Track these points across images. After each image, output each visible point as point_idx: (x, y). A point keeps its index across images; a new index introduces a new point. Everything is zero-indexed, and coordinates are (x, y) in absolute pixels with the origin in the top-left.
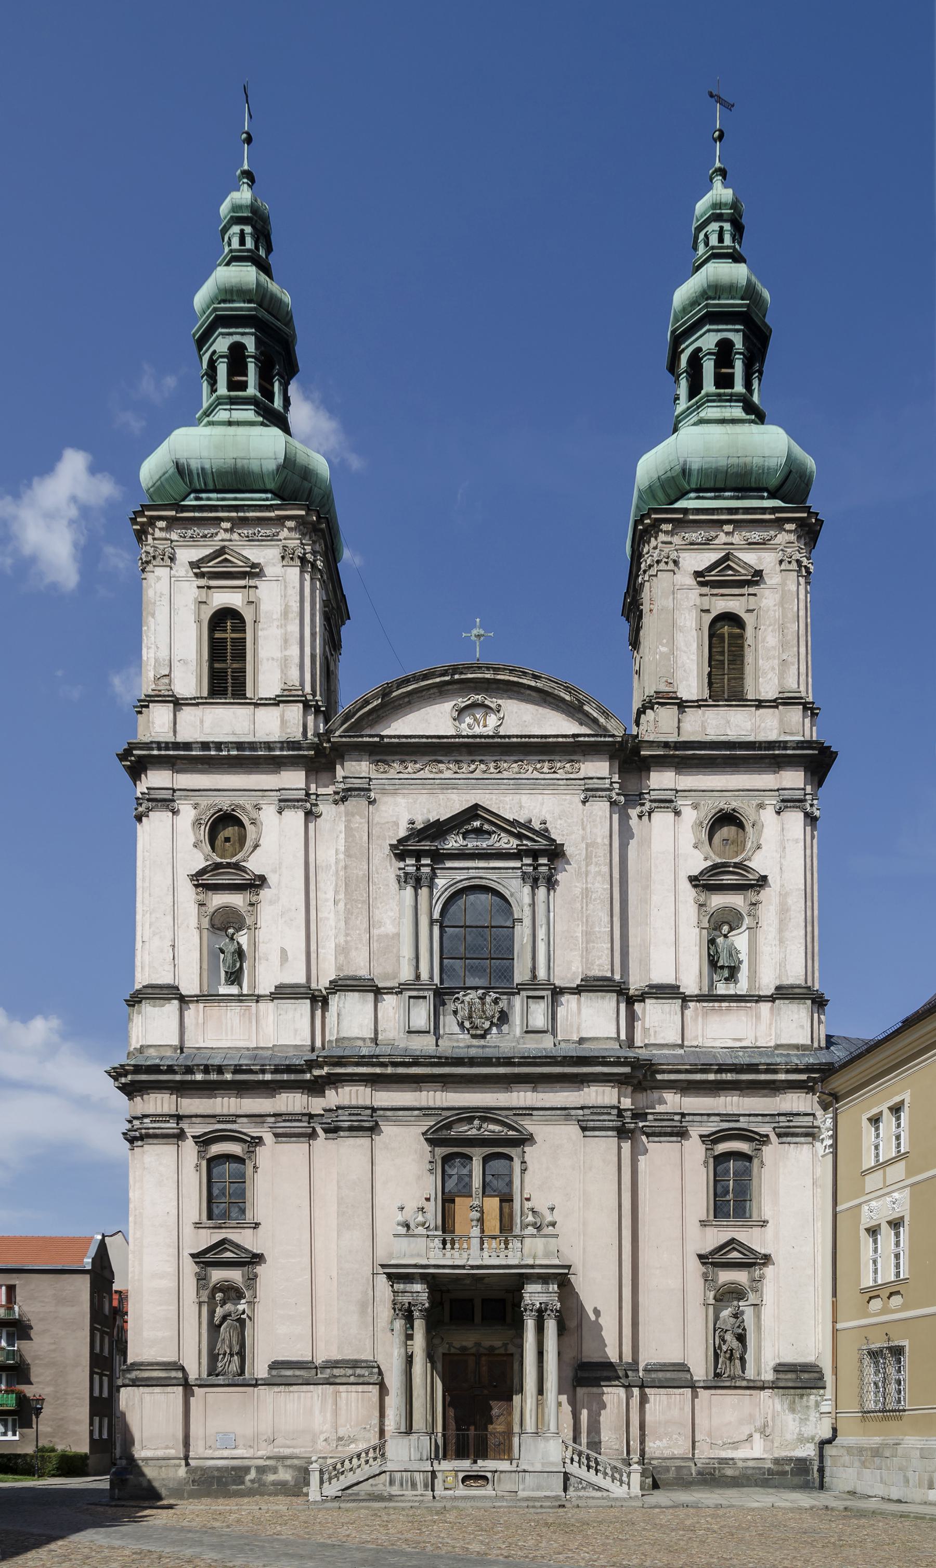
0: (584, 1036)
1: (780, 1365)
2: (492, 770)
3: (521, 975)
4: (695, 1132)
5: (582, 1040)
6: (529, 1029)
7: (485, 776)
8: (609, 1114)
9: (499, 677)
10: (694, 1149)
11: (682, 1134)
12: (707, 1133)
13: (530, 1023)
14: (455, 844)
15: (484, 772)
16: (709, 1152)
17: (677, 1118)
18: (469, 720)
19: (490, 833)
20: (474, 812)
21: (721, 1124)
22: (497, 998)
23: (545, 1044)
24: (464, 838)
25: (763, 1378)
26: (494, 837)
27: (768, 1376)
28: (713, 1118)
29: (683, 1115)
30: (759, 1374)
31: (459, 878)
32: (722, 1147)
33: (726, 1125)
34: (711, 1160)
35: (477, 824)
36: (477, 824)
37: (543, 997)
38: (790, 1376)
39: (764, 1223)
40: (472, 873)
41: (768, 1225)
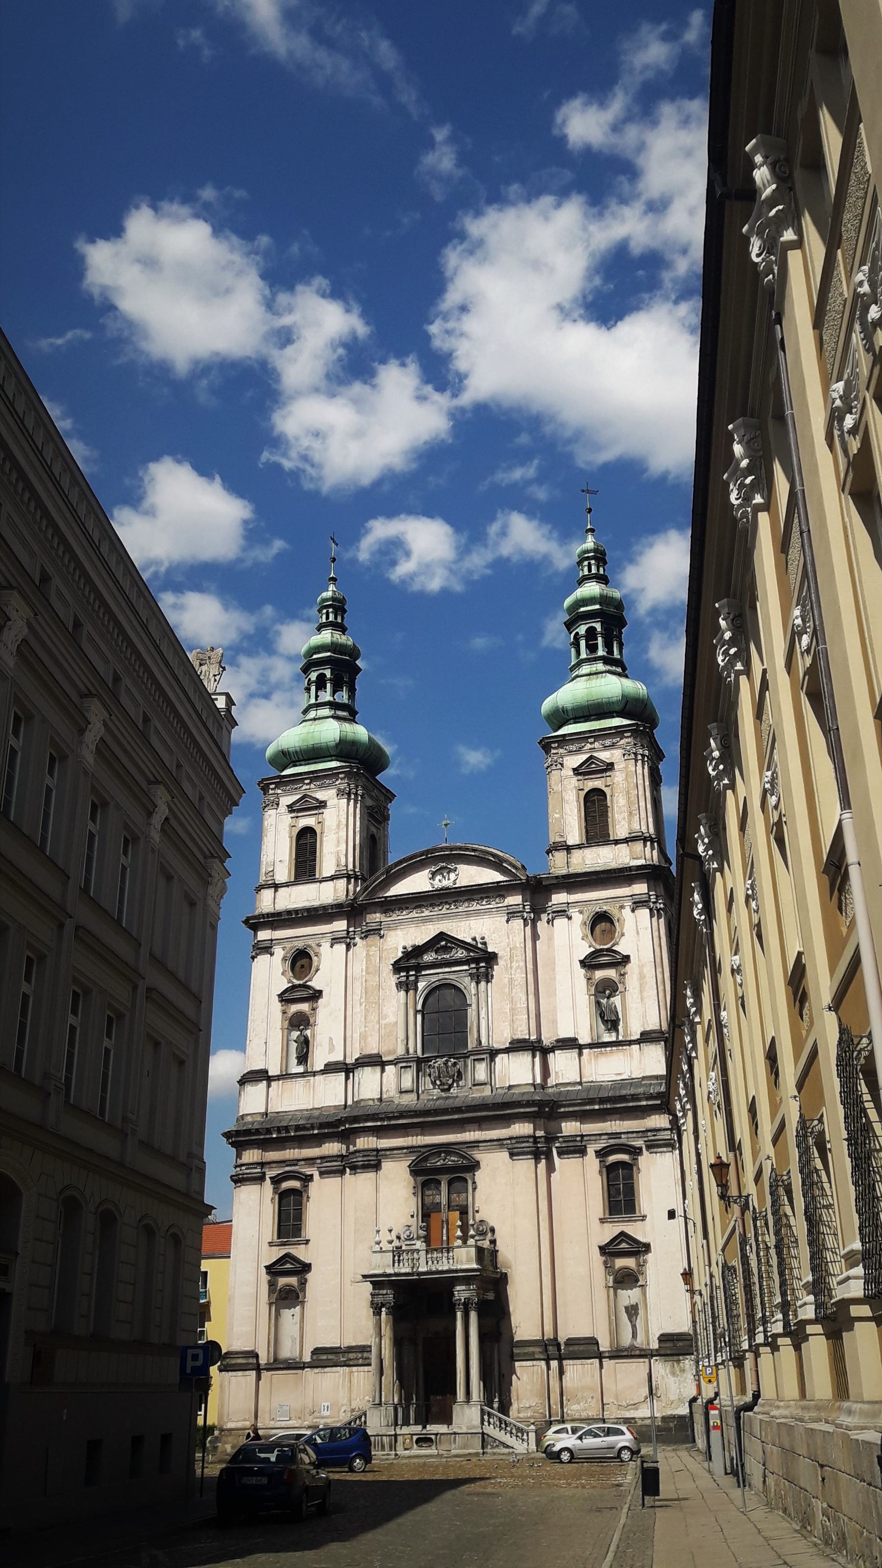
0: (512, 1084)
1: (662, 1335)
2: (453, 907)
3: (471, 1045)
4: (591, 1150)
5: (510, 1087)
6: (476, 1082)
7: (449, 912)
8: (528, 1142)
9: (453, 852)
10: (592, 1161)
11: (581, 1151)
12: (599, 1148)
13: (477, 1077)
14: (431, 958)
15: (448, 909)
16: (602, 1163)
17: (578, 1139)
18: (439, 877)
19: (452, 948)
20: (441, 936)
21: (609, 1141)
22: (455, 1062)
23: (487, 1092)
24: (436, 953)
25: (651, 1347)
26: (454, 951)
27: (655, 1345)
28: (603, 1137)
29: (582, 1136)
30: (648, 1344)
31: (433, 980)
32: (613, 1158)
33: (612, 1142)
34: (604, 1169)
35: (443, 943)
36: (443, 943)
37: (483, 1059)
38: (669, 1344)
39: (644, 1218)
40: (441, 976)
41: (647, 1219)
